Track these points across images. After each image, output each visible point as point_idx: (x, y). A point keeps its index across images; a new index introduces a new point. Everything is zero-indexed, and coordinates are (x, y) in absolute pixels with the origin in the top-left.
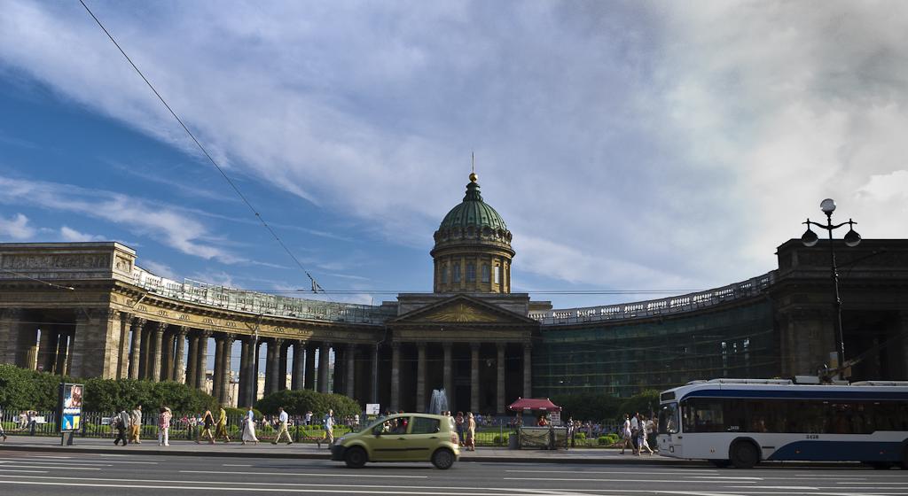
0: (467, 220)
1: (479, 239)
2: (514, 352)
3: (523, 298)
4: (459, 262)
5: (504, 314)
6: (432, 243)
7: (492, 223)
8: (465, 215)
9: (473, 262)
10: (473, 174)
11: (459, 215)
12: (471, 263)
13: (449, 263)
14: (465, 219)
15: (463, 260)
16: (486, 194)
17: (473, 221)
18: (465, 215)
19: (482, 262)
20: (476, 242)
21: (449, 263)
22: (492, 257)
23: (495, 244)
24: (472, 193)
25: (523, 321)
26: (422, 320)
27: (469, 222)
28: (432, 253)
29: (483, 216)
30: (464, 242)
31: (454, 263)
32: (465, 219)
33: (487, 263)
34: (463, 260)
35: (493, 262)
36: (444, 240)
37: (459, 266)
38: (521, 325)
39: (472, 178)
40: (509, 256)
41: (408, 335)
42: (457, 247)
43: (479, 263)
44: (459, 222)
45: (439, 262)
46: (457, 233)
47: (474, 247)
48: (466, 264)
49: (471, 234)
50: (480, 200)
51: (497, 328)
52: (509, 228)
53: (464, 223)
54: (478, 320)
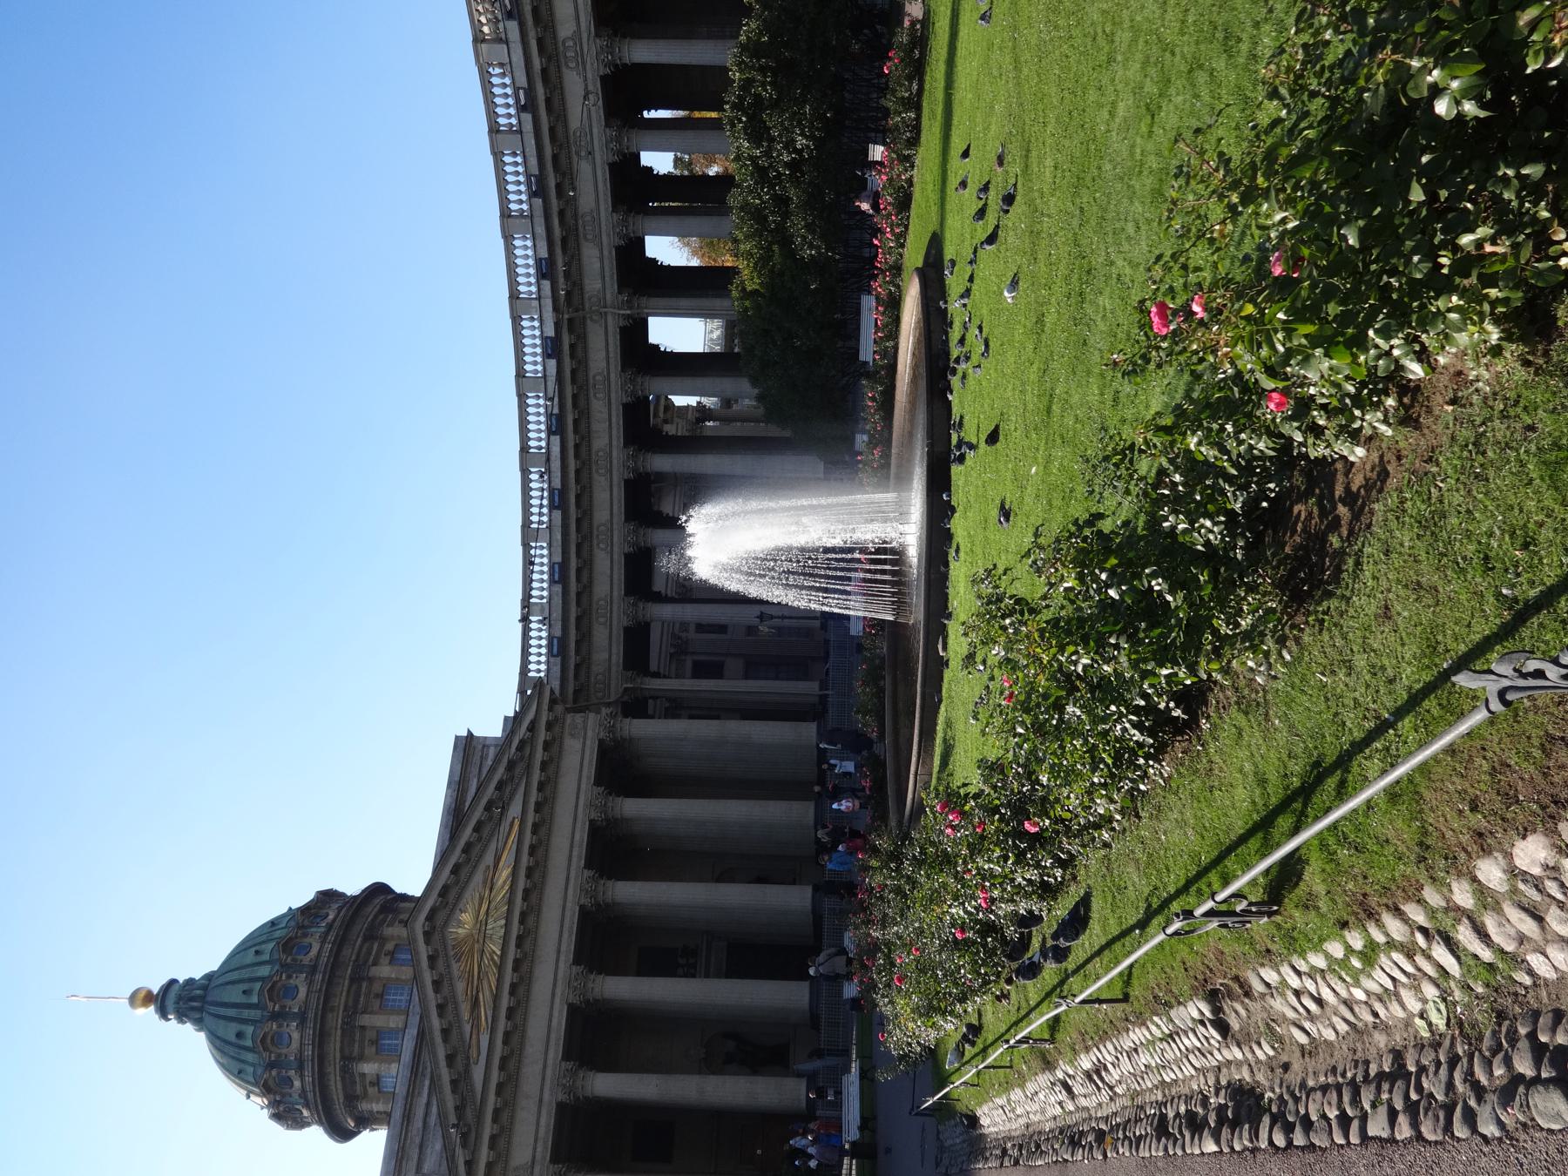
0: (249, 1006)
1: (313, 969)
2: (620, 771)
3: (467, 747)
4: (371, 1035)
5: (500, 786)
6: (315, 1134)
7: (278, 934)
8: (231, 1012)
9: (377, 988)
10: (133, 1000)
11: (229, 1031)
12: (377, 996)
13: (369, 1068)
14: (246, 1013)
15: (365, 1020)
16: (201, 955)
17: (258, 985)
18: (231, 1012)
19: (385, 960)
20: (318, 977)
21: (369, 1068)
22: (371, 935)
23: (337, 924)
24: (180, 1001)
25: (532, 728)
26: (478, 1074)
27: (255, 1000)
28: (342, 1133)
29: (250, 957)
30: (311, 1015)
31: (370, 1051)
32: (246, 1013)
33: (389, 946)
34: (365, 1020)
35: (388, 931)
36: (297, 1084)
37: (380, 1033)
38: (542, 735)
39: (148, 998)
40: (379, 901)
41: (532, 1133)
42: (321, 1037)
43: (384, 971)
44: (249, 1030)
45: (364, 1106)
46: (277, 1039)
47: (330, 982)
48: (382, 1009)
49: (291, 992)
50: (209, 977)
51: (545, 806)
52: (302, 896)
53: (254, 1014)
54: (504, 874)
